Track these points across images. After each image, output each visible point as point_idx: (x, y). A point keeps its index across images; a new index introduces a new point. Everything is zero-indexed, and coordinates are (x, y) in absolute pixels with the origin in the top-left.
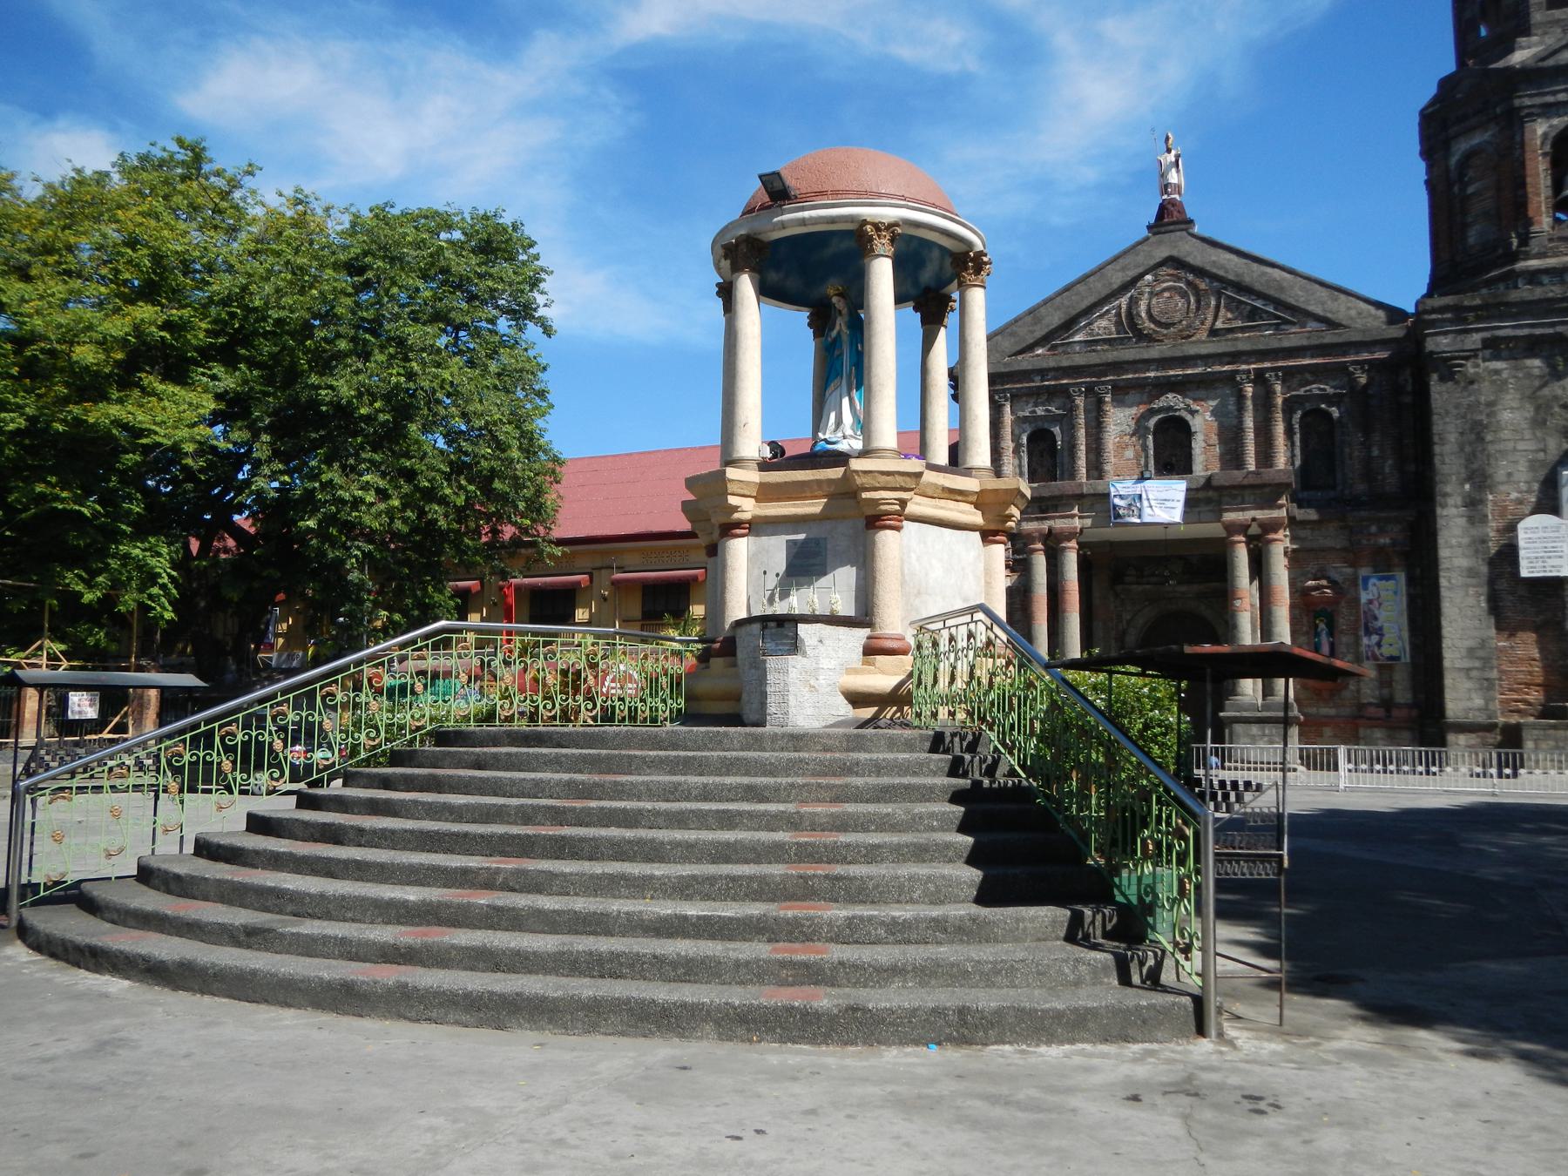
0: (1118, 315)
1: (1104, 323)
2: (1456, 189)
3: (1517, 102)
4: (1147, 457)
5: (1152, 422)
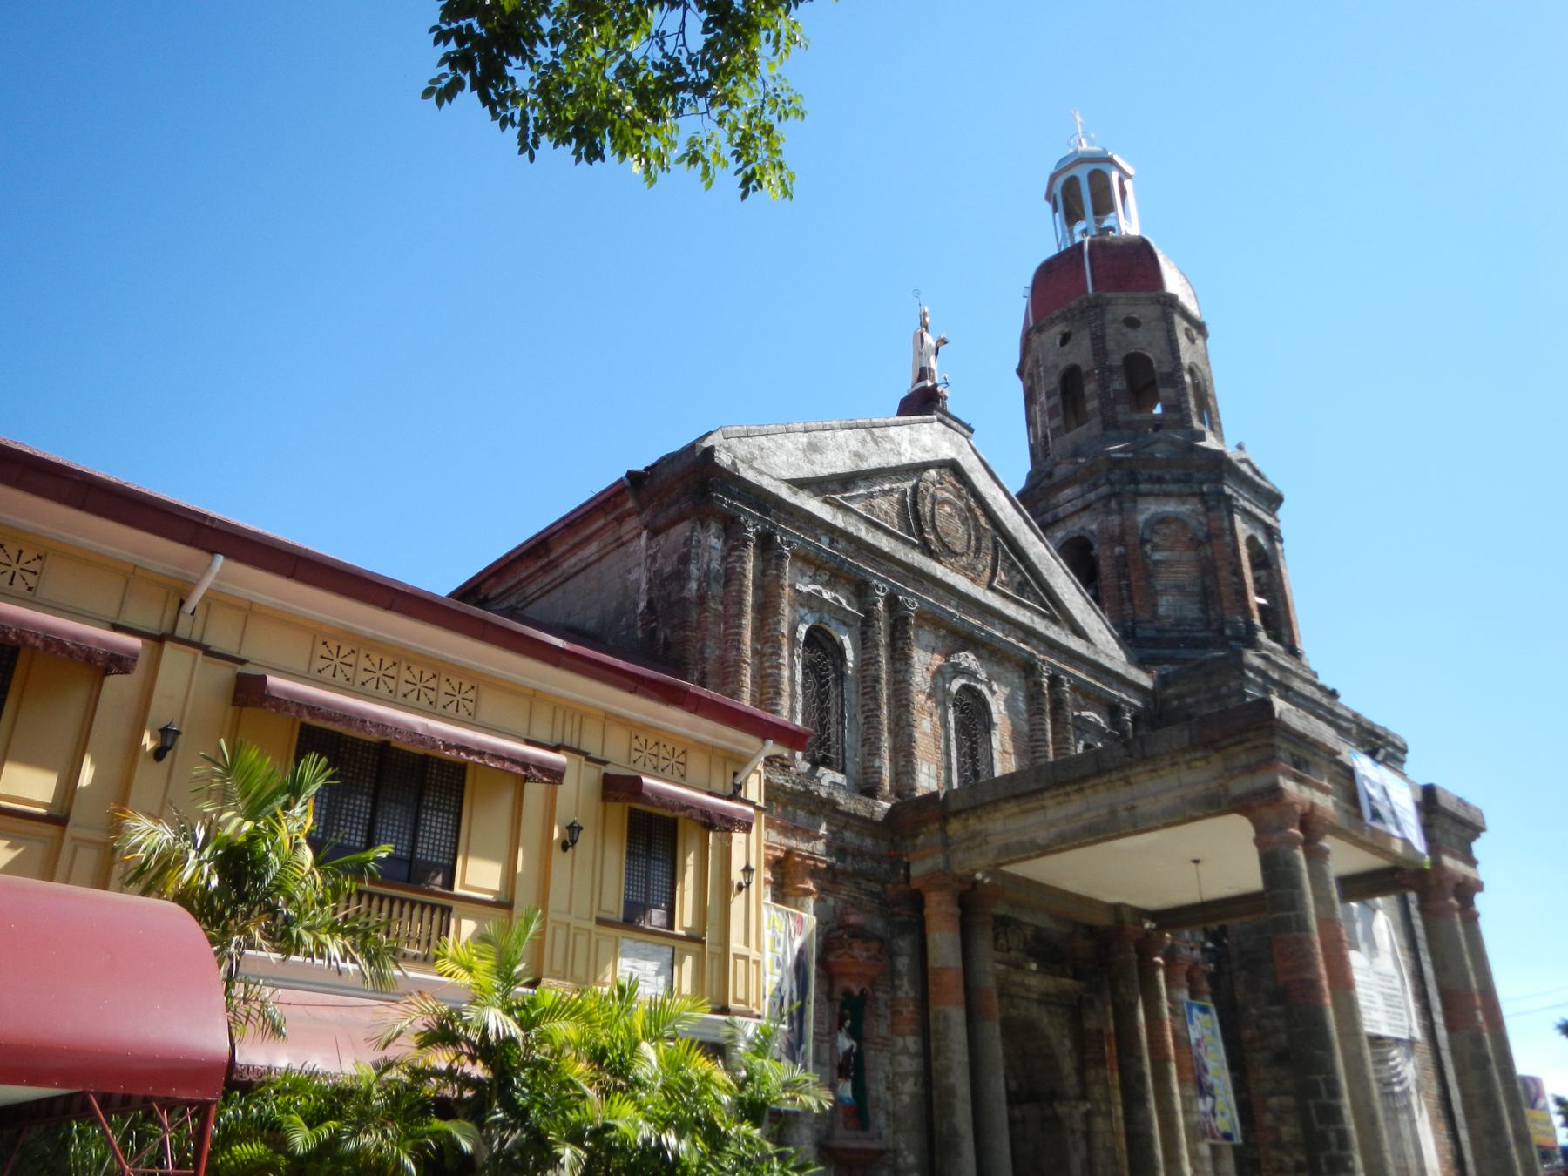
0: (902, 502)
1: (883, 504)
2: (1148, 548)
3: (1228, 491)
4: (947, 739)
5: (956, 685)
